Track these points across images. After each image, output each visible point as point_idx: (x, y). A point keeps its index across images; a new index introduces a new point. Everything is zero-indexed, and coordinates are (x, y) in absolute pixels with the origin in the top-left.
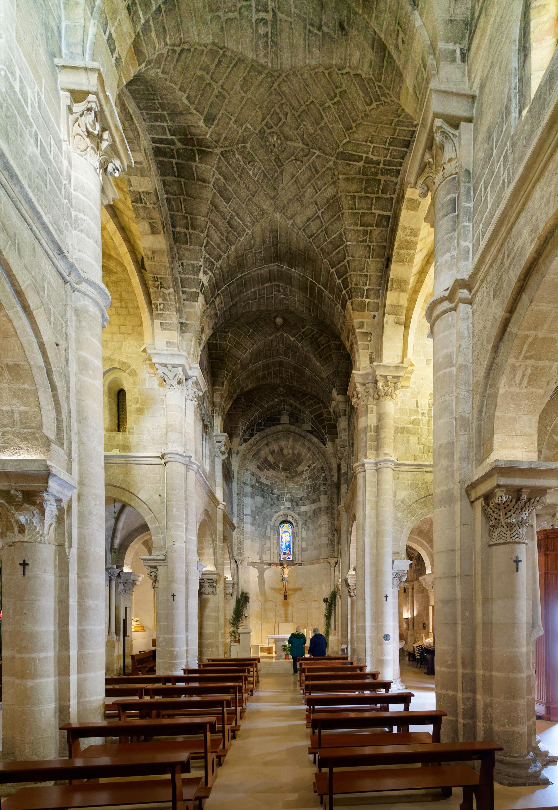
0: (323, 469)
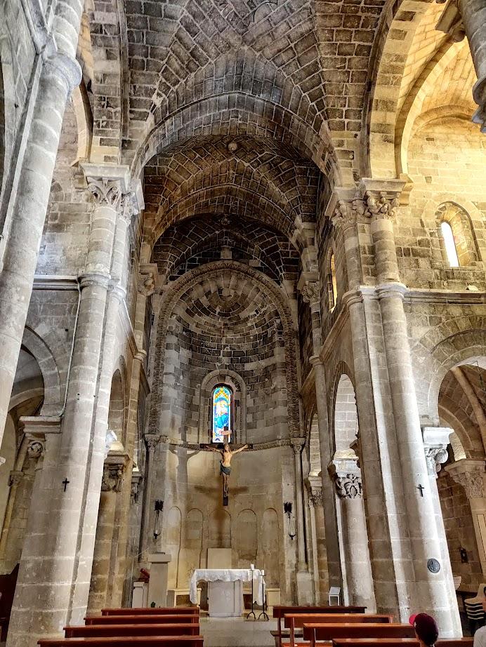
0: (277, 314)
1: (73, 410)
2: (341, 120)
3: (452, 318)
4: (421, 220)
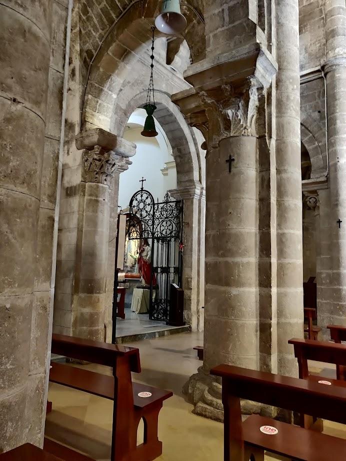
1: (336, 170)
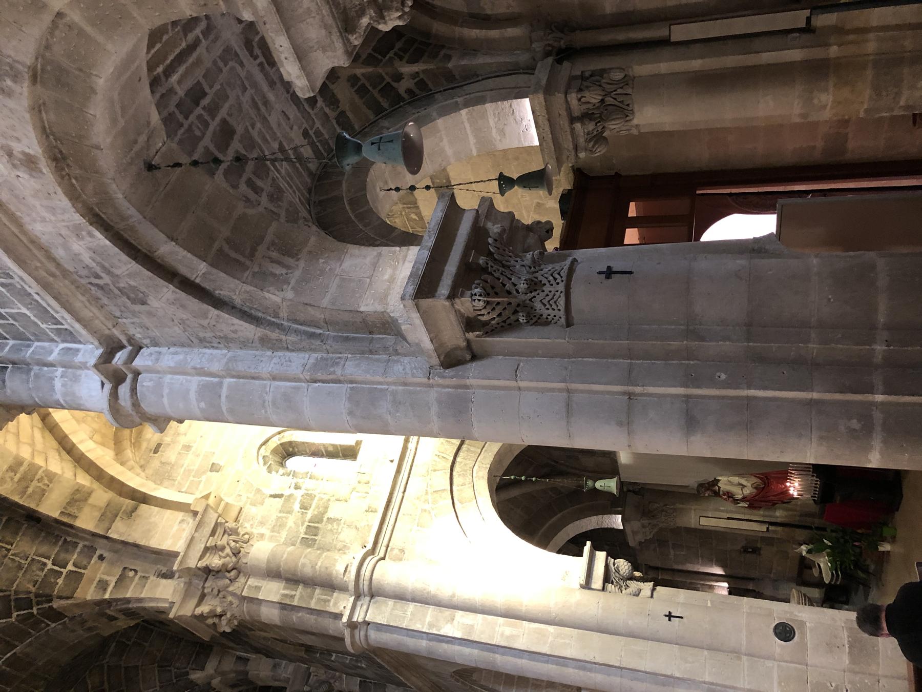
2: (63, 576)
3: (427, 493)
4: (271, 496)
